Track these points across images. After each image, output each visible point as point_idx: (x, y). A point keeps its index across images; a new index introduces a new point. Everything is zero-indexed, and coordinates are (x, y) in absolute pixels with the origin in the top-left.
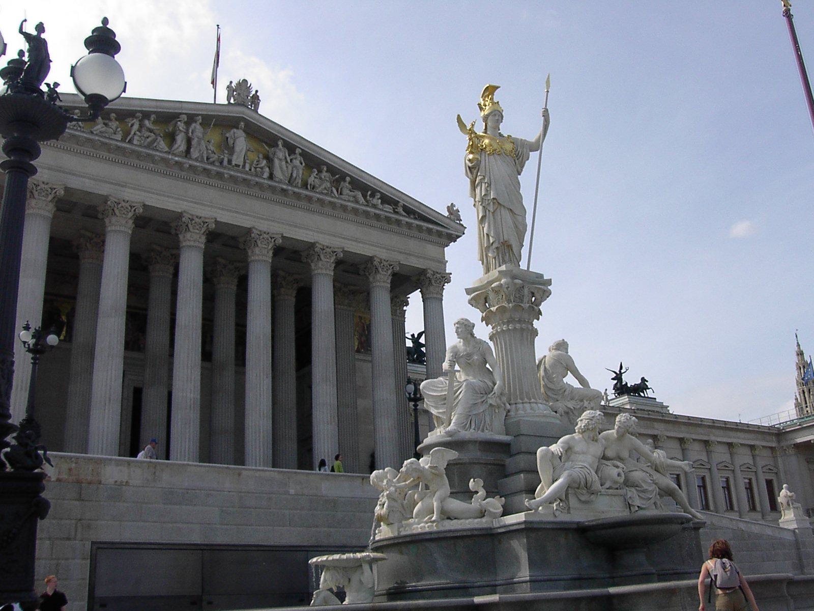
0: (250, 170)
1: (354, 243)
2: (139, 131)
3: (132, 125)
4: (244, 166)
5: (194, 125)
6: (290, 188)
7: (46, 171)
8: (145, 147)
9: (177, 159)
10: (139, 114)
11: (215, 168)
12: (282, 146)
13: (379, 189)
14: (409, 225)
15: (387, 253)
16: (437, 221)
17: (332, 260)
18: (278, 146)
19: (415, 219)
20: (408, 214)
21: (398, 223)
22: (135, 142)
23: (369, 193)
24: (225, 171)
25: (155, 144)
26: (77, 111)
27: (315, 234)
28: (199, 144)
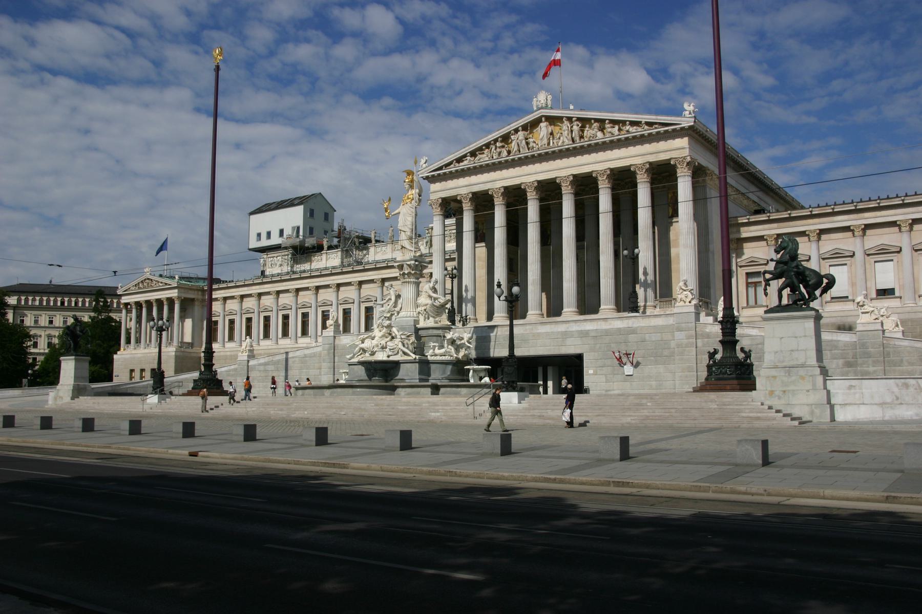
0: (553, 143)
1: (619, 161)
2: (496, 149)
3: (492, 148)
4: (549, 144)
5: (519, 133)
6: (570, 146)
7: (465, 188)
8: (498, 158)
9: (511, 158)
10: (492, 142)
11: (529, 154)
12: (566, 120)
13: (626, 119)
14: (650, 134)
15: (642, 158)
16: (672, 122)
17: (605, 177)
18: (564, 122)
19: (656, 128)
20: (649, 127)
21: (642, 136)
22: (494, 158)
23: (621, 124)
24: (535, 153)
25: (502, 154)
26: (468, 154)
27: (594, 165)
28: (521, 143)
